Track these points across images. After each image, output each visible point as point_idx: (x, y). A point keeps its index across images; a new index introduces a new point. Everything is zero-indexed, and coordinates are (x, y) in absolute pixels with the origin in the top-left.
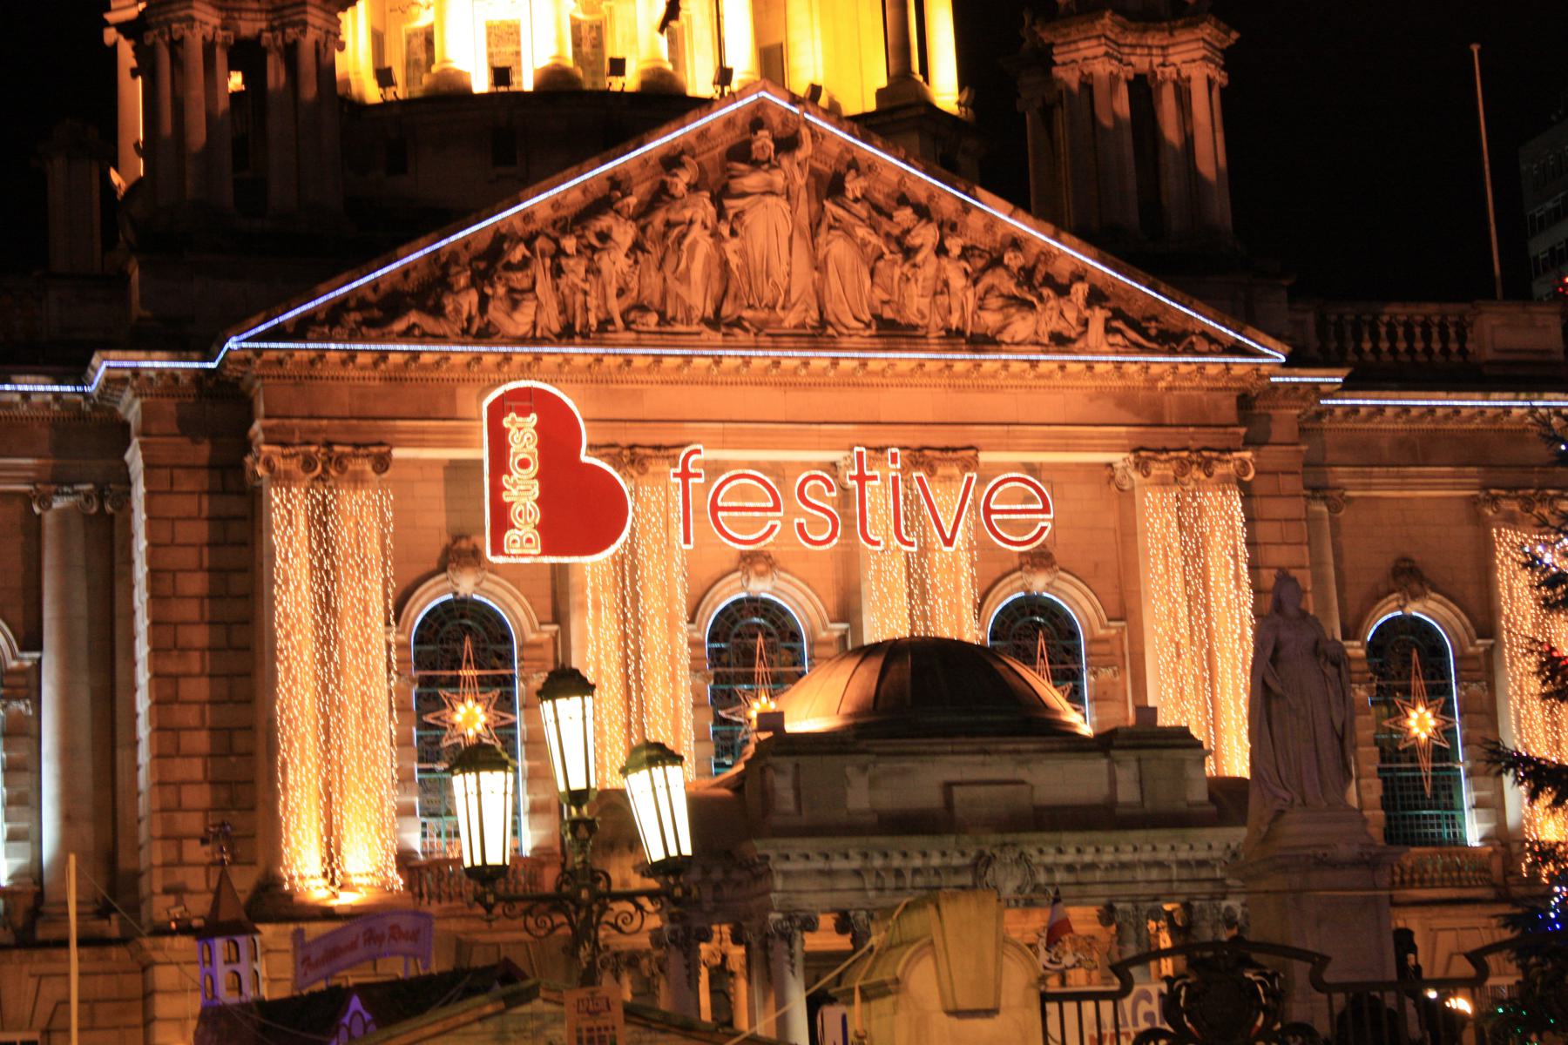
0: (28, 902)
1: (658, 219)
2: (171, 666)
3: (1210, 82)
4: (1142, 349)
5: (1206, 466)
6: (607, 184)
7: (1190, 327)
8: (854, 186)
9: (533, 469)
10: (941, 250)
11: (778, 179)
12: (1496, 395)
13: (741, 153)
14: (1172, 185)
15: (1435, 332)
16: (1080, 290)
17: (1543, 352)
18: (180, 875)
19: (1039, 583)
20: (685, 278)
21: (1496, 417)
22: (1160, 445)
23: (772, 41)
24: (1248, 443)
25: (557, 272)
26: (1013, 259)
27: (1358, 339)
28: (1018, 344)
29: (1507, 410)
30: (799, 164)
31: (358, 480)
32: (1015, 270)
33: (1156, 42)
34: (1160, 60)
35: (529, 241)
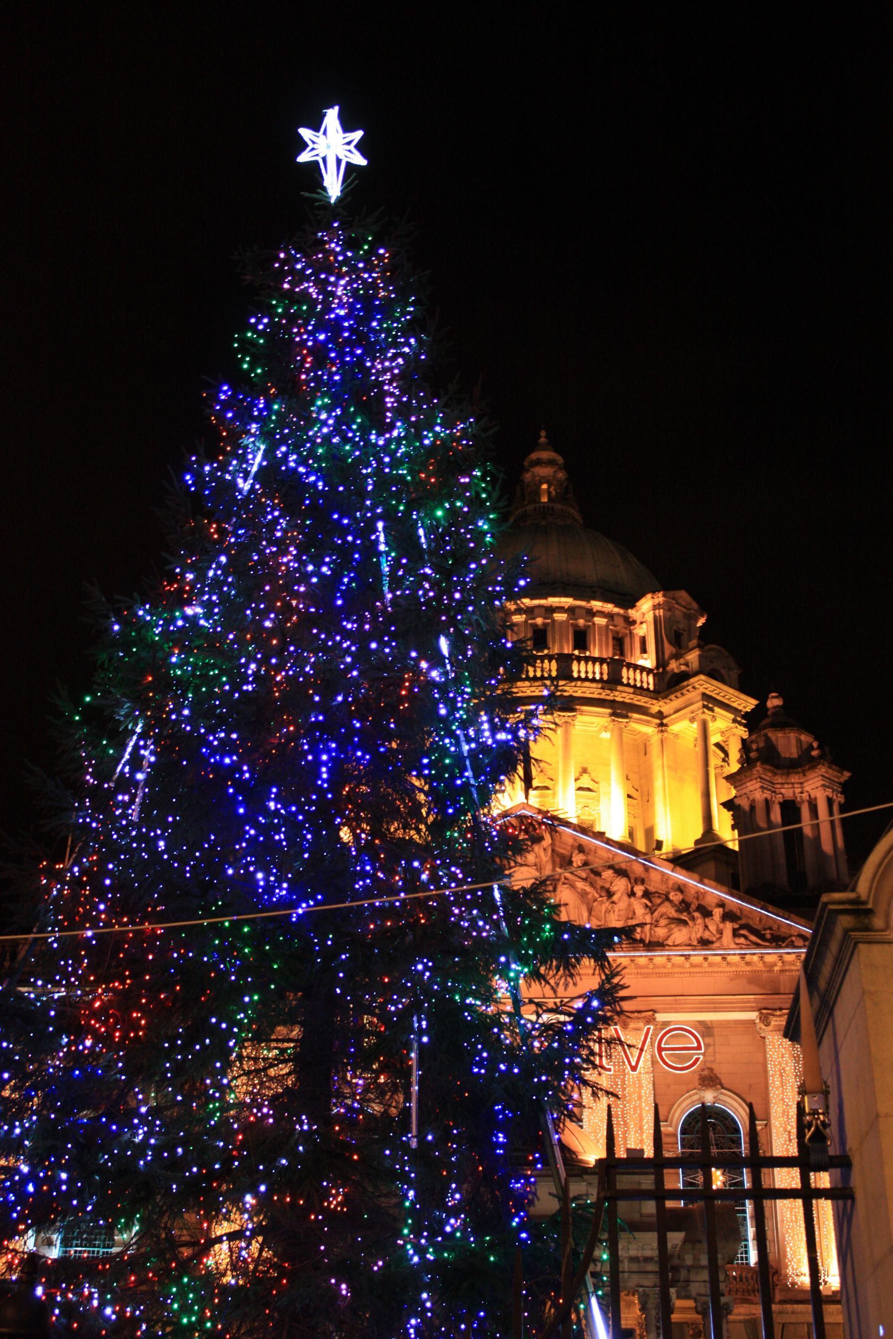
3: (830, 801)
4: (758, 946)
7: (793, 932)
8: (578, 859)
10: (632, 894)
16: (718, 912)
19: (709, 1097)
22: (776, 1006)
26: (675, 897)
28: (677, 946)
30: (545, 849)
32: (677, 903)
33: (797, 781)
34: (800, 790)
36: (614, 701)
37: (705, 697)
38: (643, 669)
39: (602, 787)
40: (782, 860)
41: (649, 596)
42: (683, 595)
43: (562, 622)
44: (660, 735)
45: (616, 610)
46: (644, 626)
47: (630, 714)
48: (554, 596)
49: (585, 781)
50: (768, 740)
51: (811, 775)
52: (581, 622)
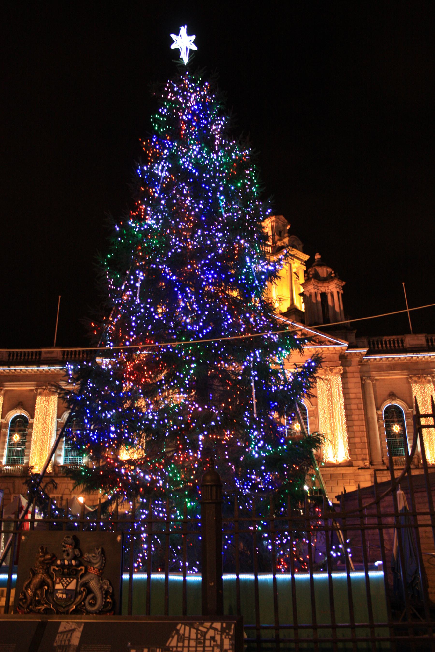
3: (338, 293)
4: (314, 345)
5: (331, 370)
7: (326, 340)
12: (408, 354)
14: (331, 313)
15: (396, 342)
17: (421, 345)
21: (410, 360)
27: (378, 344)
29: (412, 357)
40: (321, 314)
42: (282, 217)
51: (331, 283)
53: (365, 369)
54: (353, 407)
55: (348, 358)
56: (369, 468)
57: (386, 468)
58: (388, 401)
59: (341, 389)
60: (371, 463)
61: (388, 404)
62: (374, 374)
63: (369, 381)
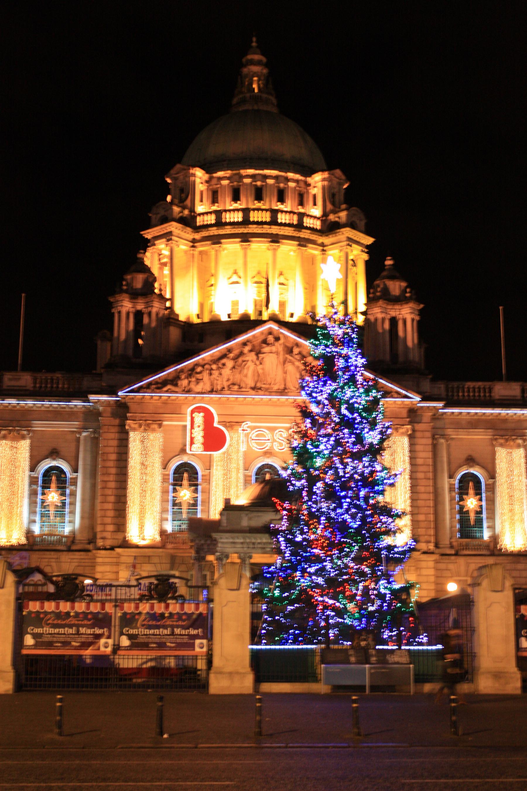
0: (71, 539)
1: (240, 360)
2: (106, 478)
3: (413, 320)
6: (226, 350)
7: (393, 390)
8: (296, 350)
9: (202, 427)
11: (274, 349)
12: (496, 409)
13: (265, 342)
14: (401, 348)
15: (482, 390)
17: (514, 396)
18: (105, 534)
20: (246, 376)
21: (497, 416)
23: (313, 304)
24: (410, 423)
25: (211, 374)
27: (458, 392)
29: (500, 414)
31: (154, 430)
34: (398, 313)
35: (203, 366)
36: (299, 237)
37: (349, 239)
38: (315, 217)
39: (290, 283)
40: (388, 348)
41: (320, 173)
42: (338, 172)
43: (271, 185)
44: (321, 256)
45: (300, 178)
46: (316, 189)
47: (307, 245)
48: (267, 169)
49: (282, 280)
50: (385, 285)
51: (405, 306)
52: (282, 185)
53: (439, 424)
54: (420, 475)
55: (419, 412)
56: (432, 553)
57: (453, 552)
58: (465, 467)
59: (407, 453)
60: (437, 546)
61: (463, 471)
62: (449, 432)
63: (442, 441)
